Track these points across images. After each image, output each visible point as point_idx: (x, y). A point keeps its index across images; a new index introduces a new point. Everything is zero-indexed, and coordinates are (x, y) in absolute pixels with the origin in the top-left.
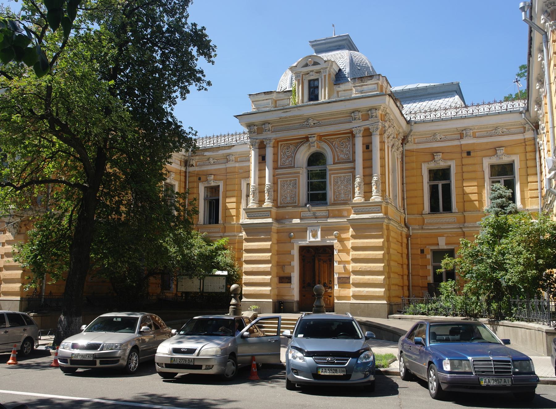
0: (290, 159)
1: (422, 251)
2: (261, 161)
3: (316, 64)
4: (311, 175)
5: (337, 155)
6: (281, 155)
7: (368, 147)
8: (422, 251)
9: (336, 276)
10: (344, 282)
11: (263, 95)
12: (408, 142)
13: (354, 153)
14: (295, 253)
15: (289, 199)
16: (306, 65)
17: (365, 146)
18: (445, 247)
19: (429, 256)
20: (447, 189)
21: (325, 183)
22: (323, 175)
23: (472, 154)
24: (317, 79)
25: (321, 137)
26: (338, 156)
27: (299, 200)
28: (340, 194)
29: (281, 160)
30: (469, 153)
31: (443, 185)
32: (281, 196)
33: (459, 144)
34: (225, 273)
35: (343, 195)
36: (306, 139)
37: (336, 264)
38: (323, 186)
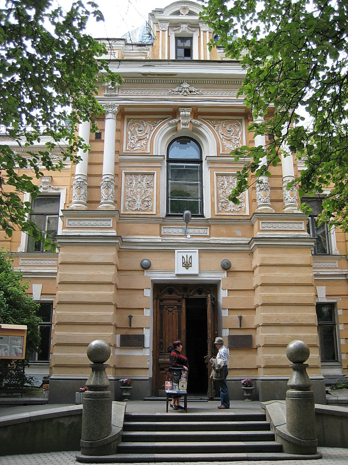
0: (144, 142)
2: (94, 138)
3: (191, 13)
5: (222, 144)
6: (127, 135)
14: (148, 293)
15: (139, 202)
16: (178, 13)
18: (325, 300)
24: (191, 38)
25: (197, 113)
26: (223, 146)
29: (127, 142)
32: (126, 196)
36: (174, 113)
37: (225, 313)
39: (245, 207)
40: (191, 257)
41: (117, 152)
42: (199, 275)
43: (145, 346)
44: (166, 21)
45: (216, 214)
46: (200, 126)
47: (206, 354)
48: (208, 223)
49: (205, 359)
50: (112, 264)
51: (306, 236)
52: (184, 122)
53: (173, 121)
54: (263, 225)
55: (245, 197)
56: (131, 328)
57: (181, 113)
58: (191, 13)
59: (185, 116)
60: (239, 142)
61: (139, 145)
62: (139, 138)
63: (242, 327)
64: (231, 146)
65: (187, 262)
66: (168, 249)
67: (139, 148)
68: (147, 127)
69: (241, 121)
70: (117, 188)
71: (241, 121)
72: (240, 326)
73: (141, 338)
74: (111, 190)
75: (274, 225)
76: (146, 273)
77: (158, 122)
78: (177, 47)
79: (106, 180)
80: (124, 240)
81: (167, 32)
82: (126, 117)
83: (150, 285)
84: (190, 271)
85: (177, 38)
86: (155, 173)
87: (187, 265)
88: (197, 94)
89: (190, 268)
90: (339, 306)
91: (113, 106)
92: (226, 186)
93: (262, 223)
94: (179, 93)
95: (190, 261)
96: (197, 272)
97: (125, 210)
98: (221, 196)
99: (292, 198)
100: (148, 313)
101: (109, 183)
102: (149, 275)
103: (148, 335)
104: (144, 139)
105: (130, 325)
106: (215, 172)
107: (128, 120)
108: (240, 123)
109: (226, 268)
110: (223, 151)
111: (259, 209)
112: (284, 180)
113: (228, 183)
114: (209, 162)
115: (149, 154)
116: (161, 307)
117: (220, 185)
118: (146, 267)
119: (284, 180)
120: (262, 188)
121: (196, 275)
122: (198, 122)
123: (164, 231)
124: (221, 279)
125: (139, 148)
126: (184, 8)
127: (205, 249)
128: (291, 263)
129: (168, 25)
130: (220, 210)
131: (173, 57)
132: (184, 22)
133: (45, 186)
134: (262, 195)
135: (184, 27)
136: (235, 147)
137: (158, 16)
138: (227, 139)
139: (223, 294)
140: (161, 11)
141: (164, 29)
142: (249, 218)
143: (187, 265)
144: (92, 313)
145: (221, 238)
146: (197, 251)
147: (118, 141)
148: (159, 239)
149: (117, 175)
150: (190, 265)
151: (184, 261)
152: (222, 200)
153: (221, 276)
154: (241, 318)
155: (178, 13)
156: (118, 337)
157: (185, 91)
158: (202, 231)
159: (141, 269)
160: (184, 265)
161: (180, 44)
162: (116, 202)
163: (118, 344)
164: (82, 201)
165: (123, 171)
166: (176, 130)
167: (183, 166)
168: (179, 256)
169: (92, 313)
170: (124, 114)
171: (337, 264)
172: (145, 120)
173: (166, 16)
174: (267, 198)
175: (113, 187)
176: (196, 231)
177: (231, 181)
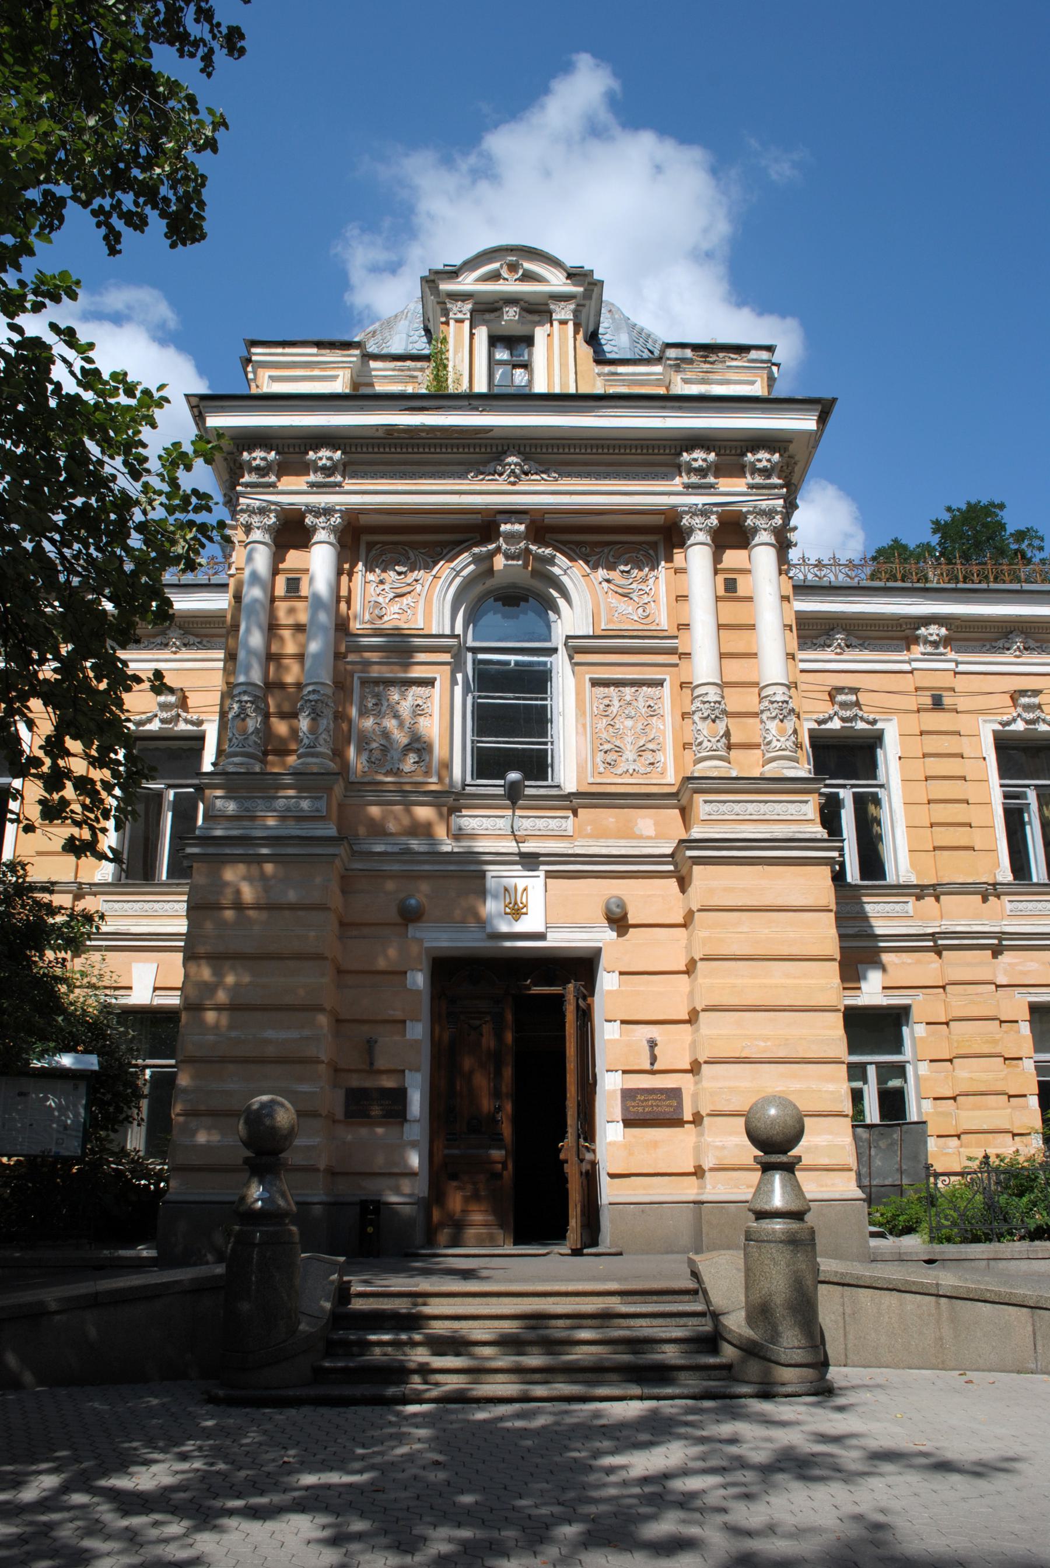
3: (529, 277)
9: (610, 1084)
11: (314, 350)
13: (682, 598)
14: (419, 980)
16: (495, 276)
17: (720, 578)
20: (865, 804)
23: (947, 701)
25: (545, 528)
28: (619, 750)
33: (906, 667)
34: (92, 1062)
35: (630, 754)
39: (665, 763)
40: (525, 889)
42: (549, 935)
43: (408, 1117)
44: (464, 297)
45: (591, 780)
46: (551, 560)
47: (562, 1136)
48: (573, 802)
49: (560, 1150)
50: (322, 908)
51: (819, 836)
54: (708, 808)
55: (664, 738)
56: (372, 1071)
57: (503, 528)
59: (511, 537)
60: (649, 599)
61: (395, 608)
62: (398, 591)
63: (656, 1067)
64: (630, 610)
65: (516, 903)
67: (396, 616)
69: (654, 545)
71: (654, 545)
72: (652, 1064)
73: (400, 1096)
74: (325, 722)
75: (737, 808)
77: (445, 552)
78: (492, 364)
79: (312, 697)
80: (355, 848)
81: (467, 323)
82: (366, 538)
83: (425, 964)
85: (494, 341)
86: (435, 679)
88: (543, 479)
89: (523, 916)
90: (915, 1014)
91: (328, 512)
92: (614, 709)
93: (706, 802)
94: (497, 477)
95: (524, 901)
96: (541, 929)
98: (604, 735)
99: (782, 739)
100: (418, 1031)
101: (320, 705)
102: (418, 935)
104: (409, 593)
105: (372, 1064)
106: (587, 677)
107: (370, 546)
108: (651, 552)
110: (609, 621)
111: (700, 766)
112: (763, 694)
113: (622, 703)
114: (573, 651)
115: (420, 632)
117: (602, 707)
118: (410, 916)
119: (763, 694)
120: (706, 715)
121: (541, 936)
124: (600, 945)
125: (396, 616)
128: (780, 902)
129: (468, 306)
130: (602, 770)
131: (481, 387)
132: (512, 300)
133: (165, 715)
134: (705, 733)
135: (511, 313)
136: (640, 610)
137: (445, 286)
138: (620, 590)
139: (607, 981)
140: (453, 273)
141: (460, 316)
142: (674, 790)
144: (270, 1034)
145: (602, 842)
146: (542, 874)
150: (524, 910)
151: (508, 901)
152: (607, 747)
153: (602, 937)
154: (653, 1044)
156: (340, 1095)
157: (513, 472)
158: (553, 824)
159: (399, 920)
160: (508, 910)
161: (502, 355)
163: (340, 1114)
164: (250, 750)
165: (356, 676)
167: (508, 663)
169: (270, 1034)
172: (413, 545)
173: (468, 283)
174: (718, 741)
175: (331, 716)
176: (541, 823)
177: (628, 698)
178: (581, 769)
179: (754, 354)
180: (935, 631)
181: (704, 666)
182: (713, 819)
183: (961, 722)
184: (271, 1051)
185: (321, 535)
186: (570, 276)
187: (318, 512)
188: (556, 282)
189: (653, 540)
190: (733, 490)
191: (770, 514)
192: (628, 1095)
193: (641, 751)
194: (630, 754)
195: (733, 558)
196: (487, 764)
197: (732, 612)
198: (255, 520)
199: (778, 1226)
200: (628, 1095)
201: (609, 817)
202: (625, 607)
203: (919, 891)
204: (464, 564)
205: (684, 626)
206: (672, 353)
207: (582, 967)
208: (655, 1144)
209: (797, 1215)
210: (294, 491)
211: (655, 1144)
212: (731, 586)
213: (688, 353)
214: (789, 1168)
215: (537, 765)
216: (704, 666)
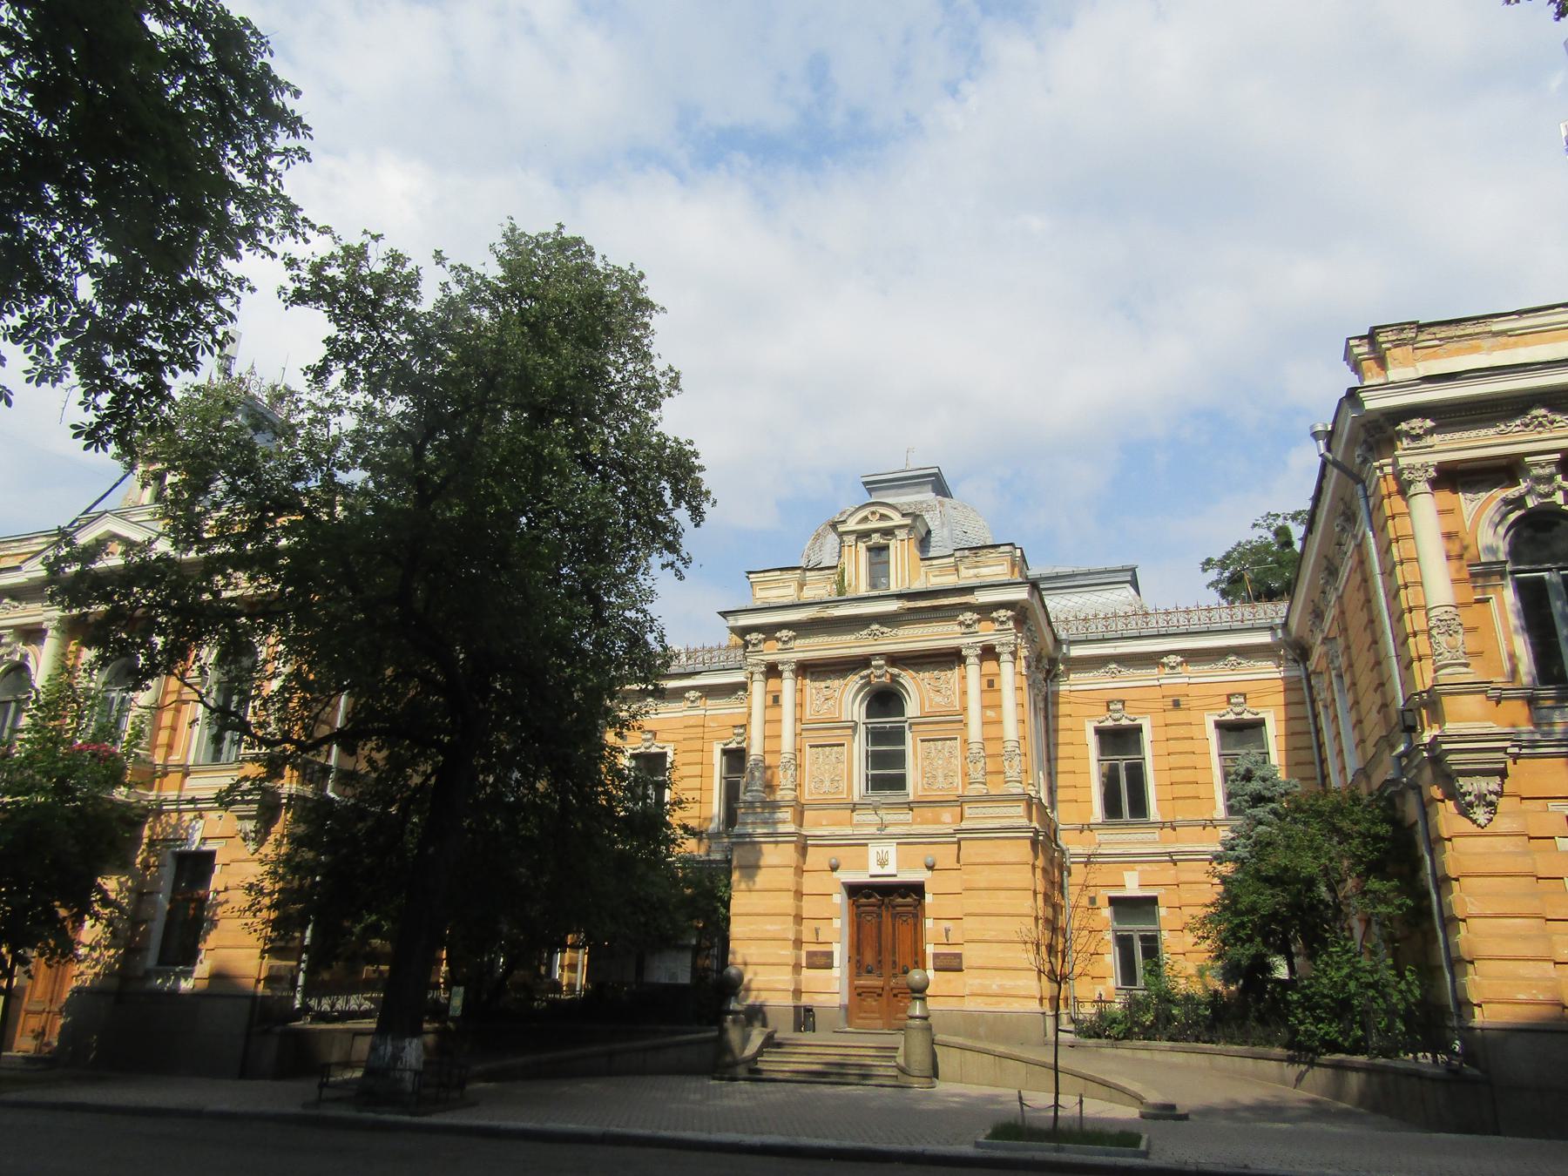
1: (1092, 900)
3: (883, 517)
4: (876, 736)
7: (991, 684)
8: (1092, 900)
9: (930, 949)
10: (950, 964)
12: (1056, 676)
13: (965, 693)
14: (840, 898)
15: (827, 783)
16: (865, 519)
19: (1107, 912)
21: (902, 754)
22: (897, 736)
24: (886, 548)
25: (895, 659)
26: (931, 700)
27: (850, 788)
28: (934, 777)
30: (1176, 704)
31: (1129, 768)
35: (941, 779)
36: (862, 662)
37: (929, 923)
38: (899, 759)
41: (798, 720)
48: (910, 806)
52: (881, 674)
53: (865, 673)
58: (883, 517)
66: (861, 843)
68: (836, 683)
70: (798, 766)
71: (953, 662)
73: (830, 955)
76: (835, 874)
84: (886, 871)
87: (882, 863)
97: (811, 793)
103: (840, 952)
109: (931, 868)
116: (858, 915)
118: (834, 868)
122: (895, 671)
123: (856, 817)
126: (873, 513)
127: (905, 841)
132: (876, 531)
137: (841, 528)
139: (928, 898)
143: (882, 863)
144: (769, 927)
147: (799, 705)
148: (848, 831)
149: (798, 750)
155: (865, 519)
162: (798, 786)
166: (869, 683)
168: (874, 850)
169: (769, 927)
170: (807, 669)
171: (1156, 836)
173: (852, 525)
178: (915, 788)
179: (1002, 549)
180: (1172, 659)
181: (975, 731)
182: (977, 817)
183: (1193, 716)
184: (768, 935)
185: (785, 675)
186: (904, 515)
187: (784, 663)
188: (897, 519)
189: (951, 658)
190: (987, 633)
191: (1007, 644)
192: (936, 956)
193: (946, 776)
194: (941, 779)
195: (990, 666)
196: (877, 783)
197: (990, 697)
198: (755, 669)
199: (918, 1022)
200: (936, 956)
201: (928, 813)
202: (938, 699)
203: (1162, 825)
204: (854, 681)
205: (965, 709)
206: (958, 554)
207: (917, 889)
208: (949, 981)
209: (925, 1018)
210: (771, 652)
211: (949, 981)
212: (991, 684)
213: (967, 553)
214: (923, 999)
215: (899, 783)
216: (975, 731)
